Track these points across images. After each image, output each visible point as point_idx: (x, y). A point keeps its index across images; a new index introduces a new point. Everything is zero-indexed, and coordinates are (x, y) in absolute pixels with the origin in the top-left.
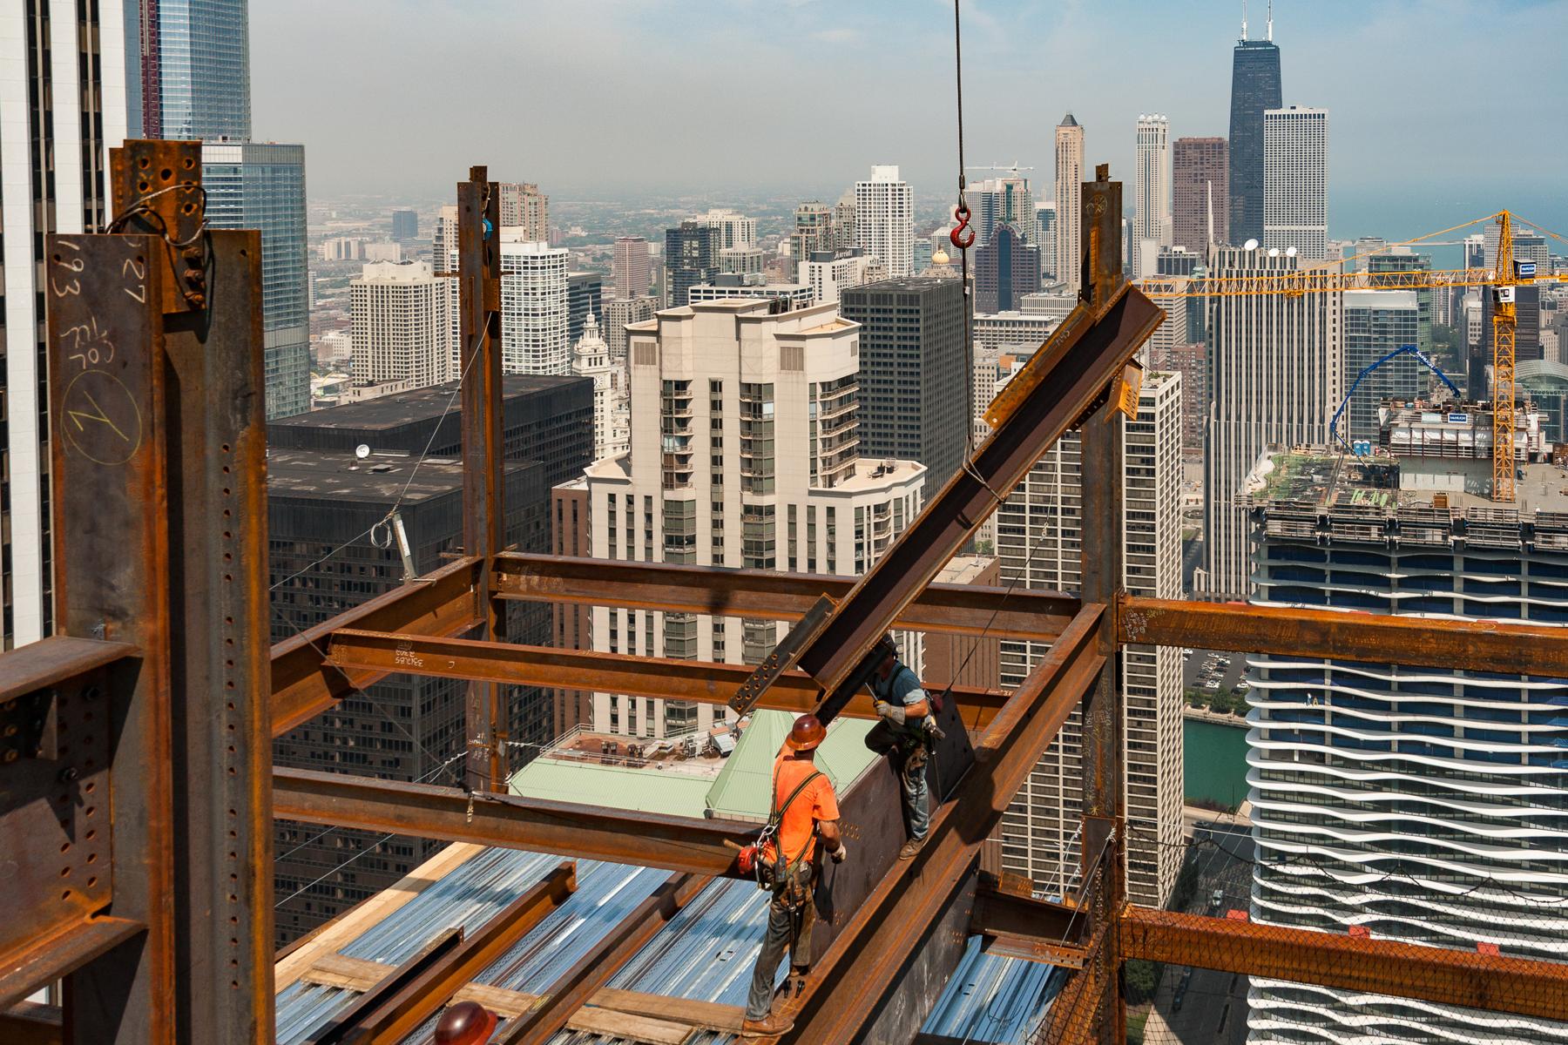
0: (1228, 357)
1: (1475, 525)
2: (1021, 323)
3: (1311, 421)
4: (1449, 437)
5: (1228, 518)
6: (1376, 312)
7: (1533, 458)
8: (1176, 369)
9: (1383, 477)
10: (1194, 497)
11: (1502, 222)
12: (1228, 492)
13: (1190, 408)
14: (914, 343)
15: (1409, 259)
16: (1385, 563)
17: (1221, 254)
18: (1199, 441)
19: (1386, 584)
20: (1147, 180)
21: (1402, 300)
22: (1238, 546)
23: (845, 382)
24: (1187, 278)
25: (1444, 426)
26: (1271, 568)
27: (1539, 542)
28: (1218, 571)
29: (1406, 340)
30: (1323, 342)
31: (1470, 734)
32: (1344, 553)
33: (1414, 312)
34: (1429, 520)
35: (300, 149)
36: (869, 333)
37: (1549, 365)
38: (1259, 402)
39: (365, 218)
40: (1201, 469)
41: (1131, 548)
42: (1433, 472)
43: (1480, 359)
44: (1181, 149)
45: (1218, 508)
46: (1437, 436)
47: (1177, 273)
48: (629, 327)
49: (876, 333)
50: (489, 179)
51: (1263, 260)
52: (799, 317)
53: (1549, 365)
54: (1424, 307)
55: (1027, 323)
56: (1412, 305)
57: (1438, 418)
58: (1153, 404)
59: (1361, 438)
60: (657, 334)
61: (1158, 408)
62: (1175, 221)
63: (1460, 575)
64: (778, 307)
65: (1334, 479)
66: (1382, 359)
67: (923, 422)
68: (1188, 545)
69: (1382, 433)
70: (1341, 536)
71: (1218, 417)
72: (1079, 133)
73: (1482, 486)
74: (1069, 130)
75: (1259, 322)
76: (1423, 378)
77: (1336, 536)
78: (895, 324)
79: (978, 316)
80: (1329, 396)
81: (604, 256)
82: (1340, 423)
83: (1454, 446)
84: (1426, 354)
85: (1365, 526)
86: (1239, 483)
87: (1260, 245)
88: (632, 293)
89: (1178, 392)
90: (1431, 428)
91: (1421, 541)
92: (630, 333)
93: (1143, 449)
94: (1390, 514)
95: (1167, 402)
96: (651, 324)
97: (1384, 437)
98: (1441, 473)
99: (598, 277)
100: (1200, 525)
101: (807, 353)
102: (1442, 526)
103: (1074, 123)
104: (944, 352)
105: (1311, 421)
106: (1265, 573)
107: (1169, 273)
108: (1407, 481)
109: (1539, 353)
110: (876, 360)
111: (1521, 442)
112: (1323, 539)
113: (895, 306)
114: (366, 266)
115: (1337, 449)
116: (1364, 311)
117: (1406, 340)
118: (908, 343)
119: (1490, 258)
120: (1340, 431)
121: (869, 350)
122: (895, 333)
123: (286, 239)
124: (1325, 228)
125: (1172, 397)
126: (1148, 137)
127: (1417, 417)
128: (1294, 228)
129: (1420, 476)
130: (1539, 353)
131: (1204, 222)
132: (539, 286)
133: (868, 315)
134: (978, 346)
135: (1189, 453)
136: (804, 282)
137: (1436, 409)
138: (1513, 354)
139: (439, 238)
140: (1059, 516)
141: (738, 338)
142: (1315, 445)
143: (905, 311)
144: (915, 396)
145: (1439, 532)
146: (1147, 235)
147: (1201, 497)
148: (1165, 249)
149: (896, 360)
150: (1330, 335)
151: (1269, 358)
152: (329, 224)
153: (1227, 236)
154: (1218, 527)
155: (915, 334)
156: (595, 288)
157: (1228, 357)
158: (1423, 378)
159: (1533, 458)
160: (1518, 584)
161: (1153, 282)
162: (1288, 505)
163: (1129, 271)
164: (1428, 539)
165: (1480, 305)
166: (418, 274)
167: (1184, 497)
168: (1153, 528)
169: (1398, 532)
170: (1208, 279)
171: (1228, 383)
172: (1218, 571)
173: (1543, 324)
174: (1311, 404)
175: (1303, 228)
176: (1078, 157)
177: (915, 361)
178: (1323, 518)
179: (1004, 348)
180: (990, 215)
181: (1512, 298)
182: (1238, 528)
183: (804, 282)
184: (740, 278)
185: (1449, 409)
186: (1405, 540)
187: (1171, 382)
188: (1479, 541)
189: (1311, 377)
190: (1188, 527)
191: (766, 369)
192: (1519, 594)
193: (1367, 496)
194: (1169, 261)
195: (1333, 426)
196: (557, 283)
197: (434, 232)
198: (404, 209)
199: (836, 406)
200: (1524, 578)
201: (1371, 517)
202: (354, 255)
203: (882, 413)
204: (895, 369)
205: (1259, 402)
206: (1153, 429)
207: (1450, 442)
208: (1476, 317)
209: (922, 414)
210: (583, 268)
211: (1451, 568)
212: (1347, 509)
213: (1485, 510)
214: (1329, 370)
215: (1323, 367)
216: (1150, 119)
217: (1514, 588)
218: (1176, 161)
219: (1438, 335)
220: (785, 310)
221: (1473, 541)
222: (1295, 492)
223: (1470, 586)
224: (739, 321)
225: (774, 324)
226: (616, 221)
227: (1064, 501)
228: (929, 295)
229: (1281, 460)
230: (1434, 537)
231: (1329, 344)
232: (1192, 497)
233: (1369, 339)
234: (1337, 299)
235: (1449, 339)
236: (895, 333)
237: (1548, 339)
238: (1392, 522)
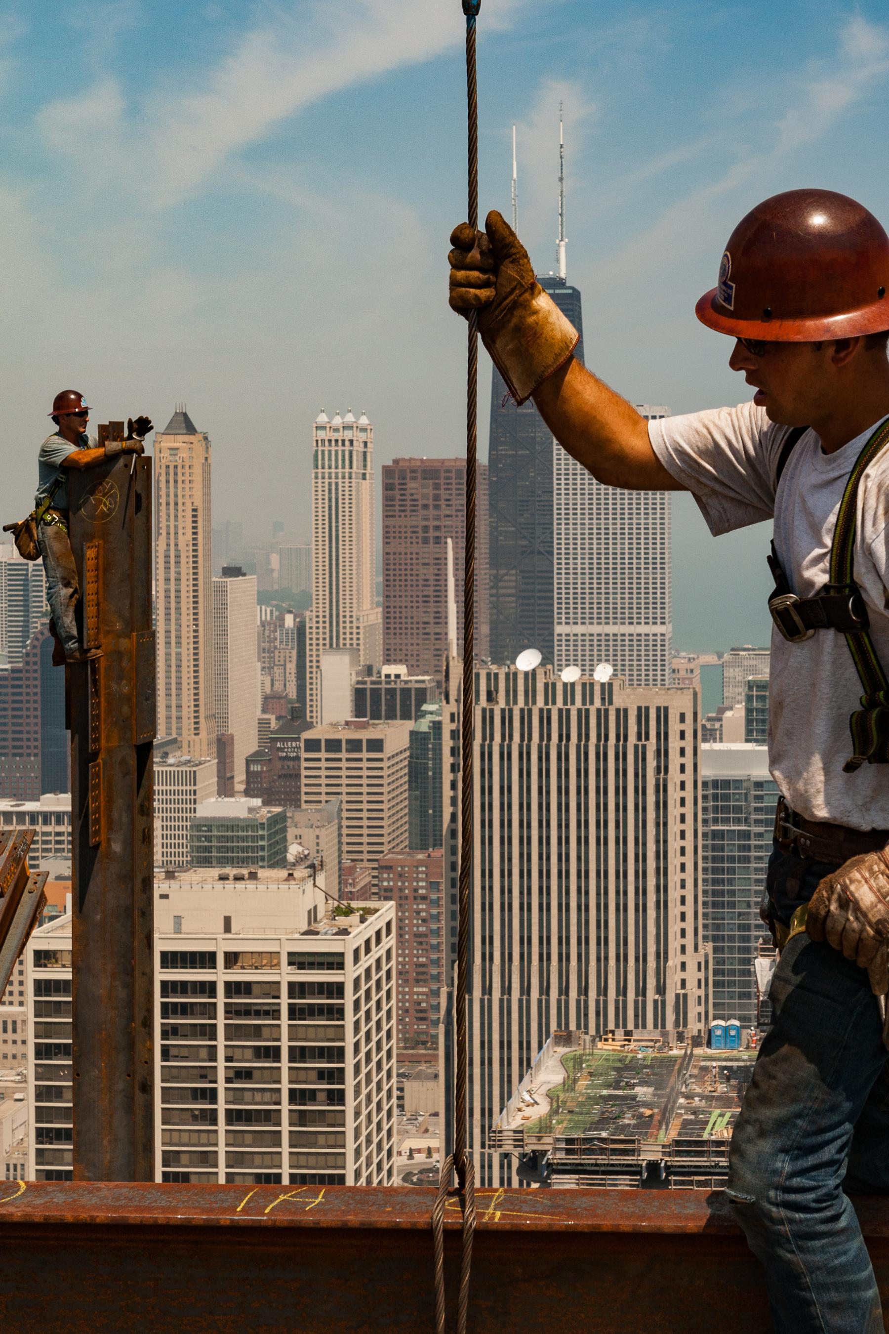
8: (387, 899)
20: (334, 539)
24: (410, 725)
30: (662, 841)
44: (398, 480)
47: (391, 716)
58: (341, 966)
62: (387, 617)
72: (199, 446)
74: (179, 441)
75: (545, 807)
87: (547, 659)
89: (389, 942)
95: (366, 961)
103: (190, 429)
107: (376, 715)
116: (738, 783)
125: (378, 952)
126: (334, 455)
128: (611, 629)
131: (441, 618)
146: (334, 644)
148: (369, 670)
150: (674, 828)
151: (564, 875)
161: (345, 735)
162: (588, 1146)
175: (627, 629)
176: (198, 493)
178: (653, 1167)
187: (376, 922)
189: (641, 909)
194: (376, 693)
206: (339, 1012)
212: (697, 1147)
214: (674, 894)
215: (662, 889)
216: (337, 421)
218: (388, 502)
222: (602, 1122)
231: (674, 844)
233: (746, 835)
234: (688, 760)
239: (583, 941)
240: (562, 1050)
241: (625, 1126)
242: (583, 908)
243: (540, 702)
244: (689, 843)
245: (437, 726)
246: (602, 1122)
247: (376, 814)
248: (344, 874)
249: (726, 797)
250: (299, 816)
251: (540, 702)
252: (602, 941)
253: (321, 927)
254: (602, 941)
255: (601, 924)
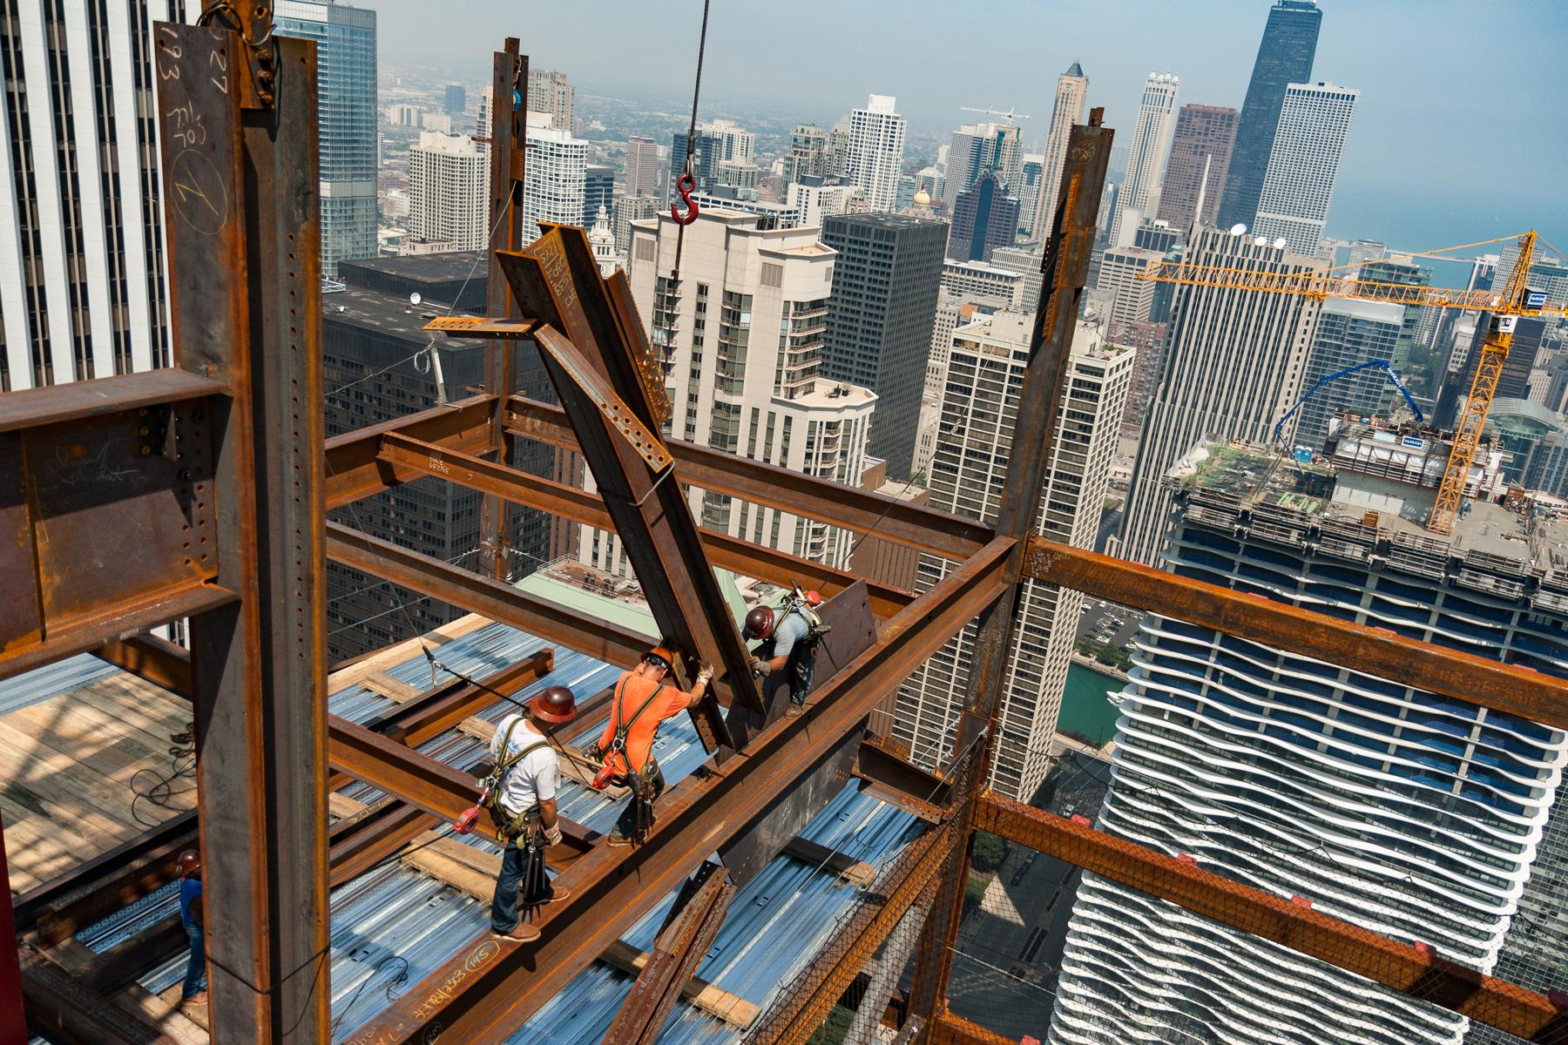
0: (1187, 342)
1: (1400, 549)
2: (988, 274)
3: (1258, 419)
4: (1396, 458)
5: (1151, 496)
6: (1355, 321)
7: (1482, 495)
9: (1320, 486)
10: (1123, 470)
11: (1525, 246)
12: (1157, 471)
13: (1137, 386)
14: (884, 279)
15: (1407, 270)
16: (1298, 566)
17: (1205, 235)
18: (1139, 418)
19: (1293, 585)
21: (1388, 312)
22: (1156, 523)
23: (816, 304)
25: (1396, 448)
26: (1182, 549)
27: (1463, 578)
28: (1131, 542)
29: (1380, 354)
31: (1338, 734)
32: (1259, 549)
33: (1396, 327)
34: (1354, 535)
35: (371, 14)
36: (844, 262)
37: (1530, 407)
38: (1208, 391)
39: (423, 88)
40: (1136, 445)
41: (1052, 505)
42: (1372, 490)
43: (1456, 387)
45: (1144, 485)
46: (1385, 456)
48: (634, 222)
49: (851, 263)
50: (521, 52)
51: (1247, 248)
52: (783, 236)
53: (1530, 407)
54: (1409, 323)
55: (994, 276)
56: (1397, 320)
57: (1392, 438)
59: (1304, 444)
60: (657, 232)
61: (1107, 379)
63: (1370, 591)
64: (765, 223)
65: (1266, 479)
66: (1346, 367)
67: (881, 355)
68: (1107, 513)
69: (1328, 443)
70: (1259, 533)
71: (1164, 399)
73: (1420, 513)
75: (1228, 312)
76: (1387, 397)
77: (1254, 532)
78: (870, 258)
79: (948, 262)
80: (1282, 398)
81: (619, 153)
82: (1287, 426)
83: (1401, 469)
84: (1398, 373)
85: (1286, 529)
86: (1170, 465)
87: (1248, 232)
88: (639, 192)
89: (1129, 368)
90: (1382, 447)
91: (1339, 553)
92: (634, 228)
93: (1083, 416)
94: (1314, 522)
95: (1116, 375)
96: (652, 223)
97: (1330, 448)
98: (1379, 492)
99: (610, 171)
100: (1123, 497)
101: (786, 272)
102: (1365, 544)
104: (910, 292)
105: (1258, 419)
106: (1176, 552)
108: (1341, 494)
109: (1524, 392)
110: (847, 289)
111: (1475, 478)
112: (1240, 532)
113: (872, 240)
114: (423, 134)
115: (1277, 450)
116: (1342, 317)
117: (1380, 354)
118: (879, 278)
119: (1498, 284)
120: (1285, 434)
121: (842, 279)
122: (868, 266)
123: (360, 100)
124: (1323, 223)
125: (1122, 372)
127: (1369, 433)
128: (1289, 218)
129: (1356, 492)
130: (1524, 392)
132: (562, 173)
133: (846, 245)
134: (943, 291)
135: (1128, 429)
136: (791, 204)
137: (1392, 430)
138: (1493, 388)
139: (482, 116)
140: (992, 464)
141: (726, 248)
142: (1256, 443)
143: (880, 246)
144: (877, 329)
145: (1361, 548)
147: (1130, 471)
149: (865, 292)
152: (395, 90)
153: (1215, 217)
154: (1139, 502)
155: (886, 270)
156: (608, 182)
157: (1187, 342)
158: (1387, 397)
159: (1482, 495)
160: (1429, 613)
162: (1213, 494)
163: (1105, 239)
164: (1348, 553)
165: (1472, 331)
166: (462, 147)
167: (1113, 468)
168: (1077, 491)
169: (1318, 541)
170: (1185, 259)
171: (1182, 368)
172: (1131, 542)
173: (1538, 362)
174: (1262, 402)
177: (883, 296)
178: (1245, 513)
179: (968, 297)
180: (977, 161)
181: (1511, 329)
182: (1159, 507)
183: (791, 204)
184: (735, 191)
185: (1406, 432)
186: (1323, 549)
187: (1125, 357)
188: (1399, 565)
189: (1269, 376)
190: (1111, 496)
191: (748, 281)
192: (1426, 622)
193: (1296, 501)
195: (1279, 427)
196: (575, 172)
197: (479, 110)
198: (455, 84)
199: (805, 325)
200: (1437, 609)
201: (1295, 521)
202: (414, 123)
203: (846, 340)
204: (864, 301)
205: (1208, 391)
206: (1096, 398)
207: (1398, 465)
208: (1464, 343)
209: (882, 347)
210: (600, 162)
211: (1363, 585)
212: (1273, 509)
213: (1416, 537)
214: (1289, 372)
215: (1283, 368)
217: (1423, 616)
219: (1416, 355)
220: (771, 227)
221: (1394, 564)
222: (1223, 485)
223: (1377, 604)
224: (729, 231)
225: (759, 239)
226: (632, 120)
227: (999, 450)
228: (905, 233)
229: (1216, 451)
230: (1355, 552)
231: (1296, 345)
232: (1122, 470)
233: (1339, 347)
235: (1427, 364)
236: (868, 266)
237: (1539, 380)
238: (1315, 530)
239: (1232, 387)
240: (1209, 443)
241: (1234, 490)
242: (1236, 370)
243: (1239, 254)
244: (1305, 346)
245: (1178, 259)
246: (1223, 485)
247: (1135, 300)
248: (1112, 327)
249: (1333, 324)
250: (1094, 293)
251: (1239, 254)
252: (1242, 389)
253: (1097, 353)
254: (1242, 389)
255: (1245, 380)
